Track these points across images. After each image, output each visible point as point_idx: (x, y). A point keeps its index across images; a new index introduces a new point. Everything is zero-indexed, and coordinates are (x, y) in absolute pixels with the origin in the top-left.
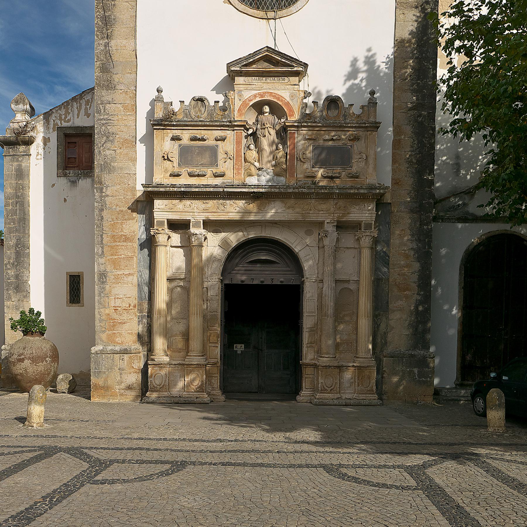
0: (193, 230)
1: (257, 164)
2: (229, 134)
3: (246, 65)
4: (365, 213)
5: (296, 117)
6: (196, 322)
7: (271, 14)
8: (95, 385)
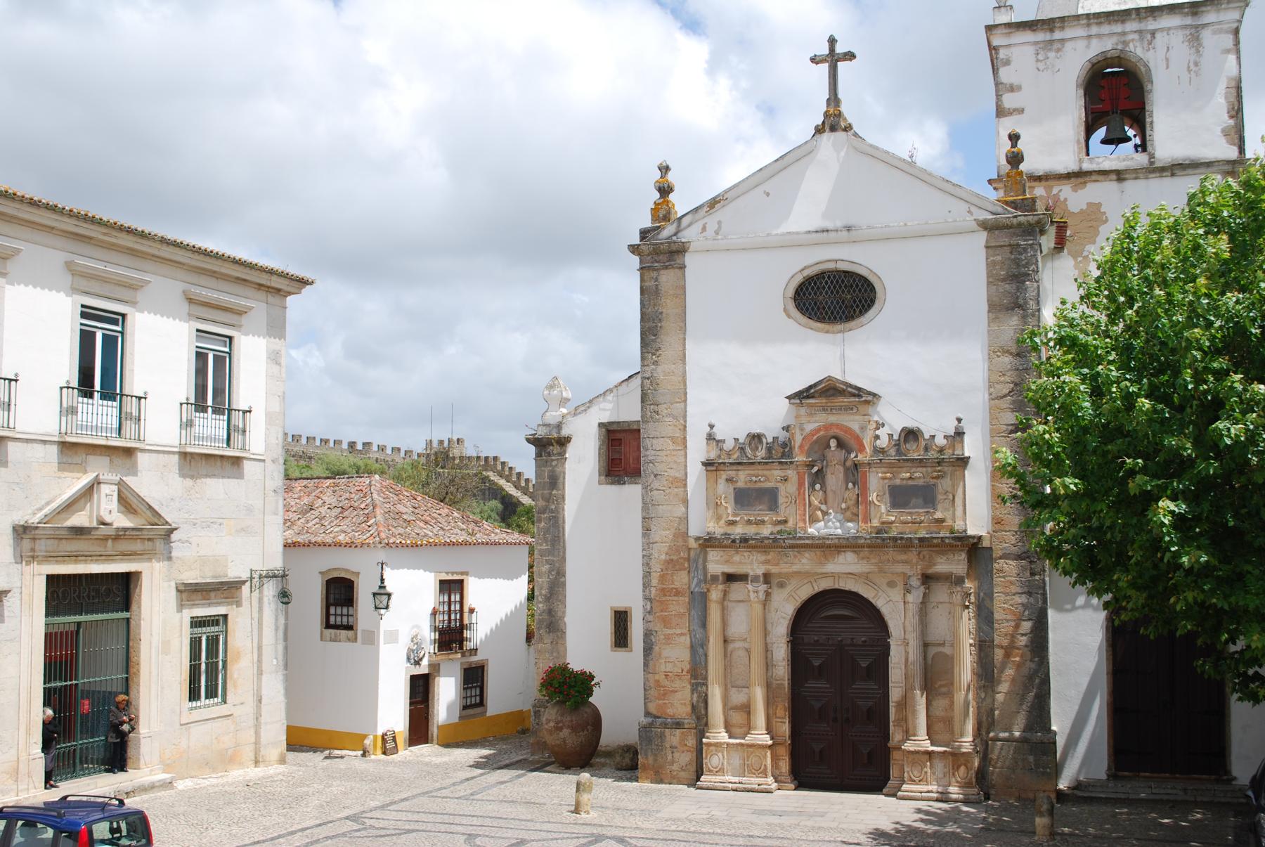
2: (791, 473)
3: (808, 397)
6: (759, 695)
8: (644, 765)
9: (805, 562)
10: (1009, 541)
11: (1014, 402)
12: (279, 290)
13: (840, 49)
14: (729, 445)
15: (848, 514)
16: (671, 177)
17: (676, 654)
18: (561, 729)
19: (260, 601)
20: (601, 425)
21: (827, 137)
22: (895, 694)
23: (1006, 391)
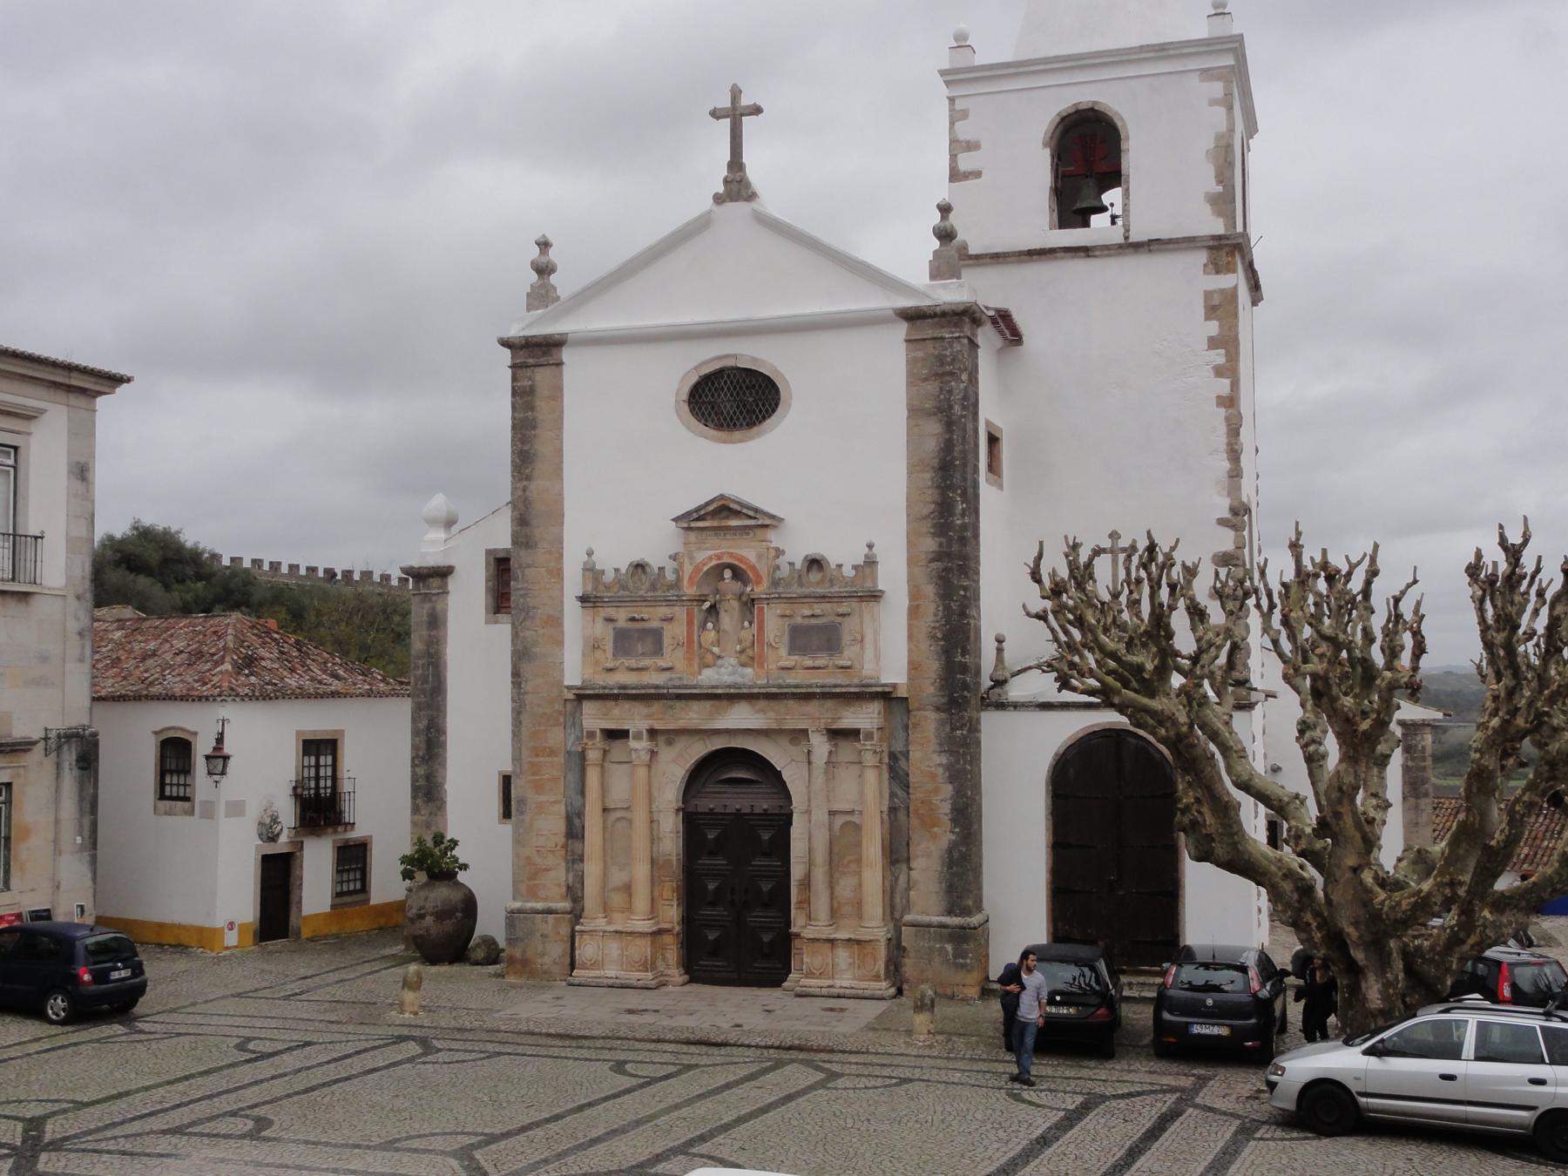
0: (633, 744)
1: (715, 650)
2: (680, 612)
4: (865, 717)
5: (765, 585)
6: (642, 871)
7: (737, 434)
9: (693, 716)
10: (929, 689)
11: (934, 526)
12: (83, 391)
13: (745, 101)
14: (609, 577)
15: (743, 658)
16: (553, 254)
17: (552, 826)
18: (422, 917)
19: (58, 766)
20: (489, 552)
21: (730, 206)
22: (797, 872)
23: (925, 511)
